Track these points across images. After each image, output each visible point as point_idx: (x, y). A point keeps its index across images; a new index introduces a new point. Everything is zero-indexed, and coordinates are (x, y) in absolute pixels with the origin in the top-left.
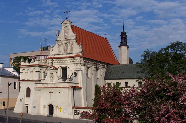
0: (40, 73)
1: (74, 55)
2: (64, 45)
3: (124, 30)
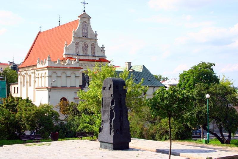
1: (97, 59)
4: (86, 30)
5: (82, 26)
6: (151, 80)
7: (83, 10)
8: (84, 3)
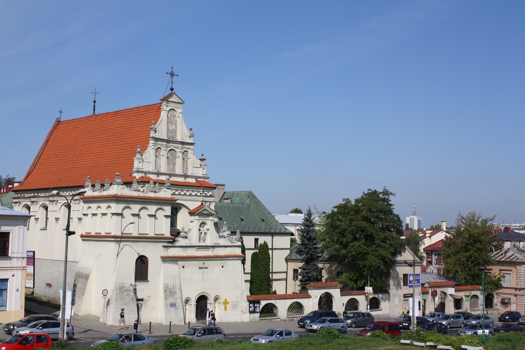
0: (156, 218)
1: (192, 181)
3: (94, 110)
4: (174, 125)
6: (265, 220)
7: (170, 87)
8: (172, 74)
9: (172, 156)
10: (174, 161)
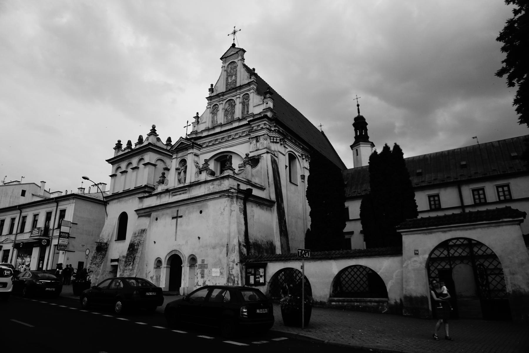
2: (227, 105)
5: (227, 72)
9: (230, 107)
10: (233, 110)
